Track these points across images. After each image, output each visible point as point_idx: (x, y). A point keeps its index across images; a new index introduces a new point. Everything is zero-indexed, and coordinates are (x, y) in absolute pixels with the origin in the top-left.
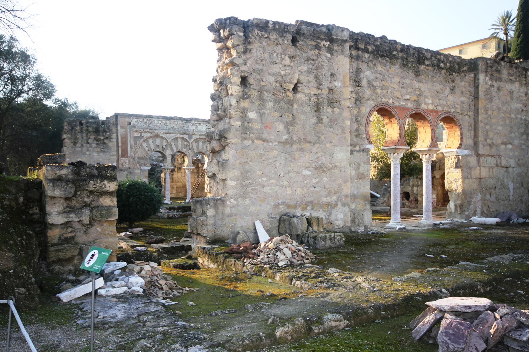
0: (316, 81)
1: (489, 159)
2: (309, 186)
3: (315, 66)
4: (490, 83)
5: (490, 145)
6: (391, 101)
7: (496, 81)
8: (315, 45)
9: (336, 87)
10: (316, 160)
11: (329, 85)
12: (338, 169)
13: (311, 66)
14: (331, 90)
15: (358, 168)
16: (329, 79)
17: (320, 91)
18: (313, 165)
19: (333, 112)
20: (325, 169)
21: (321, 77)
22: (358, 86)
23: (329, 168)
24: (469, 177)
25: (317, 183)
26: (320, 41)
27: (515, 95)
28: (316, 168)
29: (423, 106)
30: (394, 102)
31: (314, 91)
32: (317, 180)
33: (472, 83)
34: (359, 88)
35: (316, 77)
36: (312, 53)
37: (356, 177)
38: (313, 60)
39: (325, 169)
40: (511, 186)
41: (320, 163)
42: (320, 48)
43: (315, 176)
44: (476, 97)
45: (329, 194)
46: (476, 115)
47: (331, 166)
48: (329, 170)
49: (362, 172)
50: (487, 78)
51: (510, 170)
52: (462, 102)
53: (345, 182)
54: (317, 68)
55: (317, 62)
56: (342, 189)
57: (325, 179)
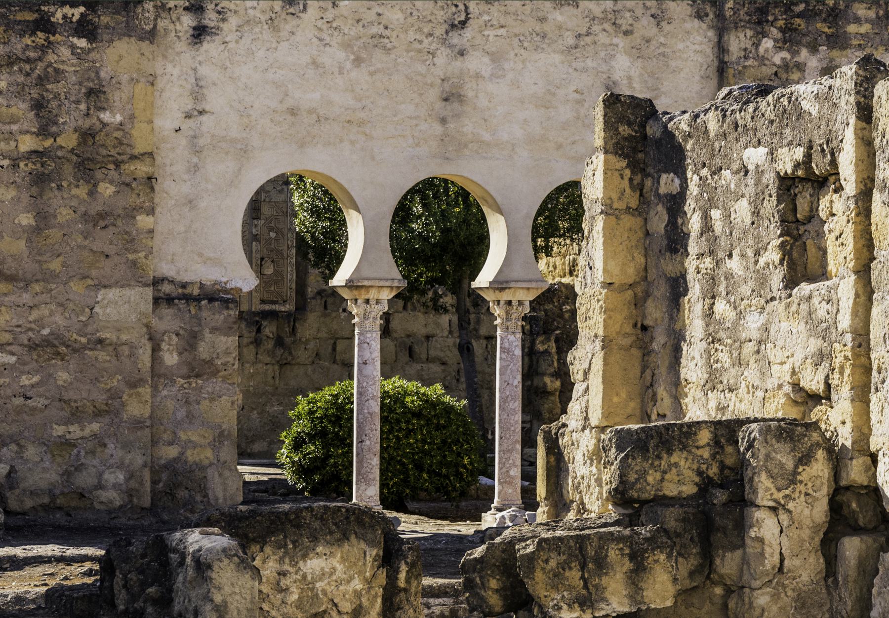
0: (37, 115)
3: (35, 75)
8: (36, 21)
11: (80, 123)
12: (111, 349)
13: (21, 79)
14: (87, 135)
16: (83, 107)
17: (48, 143)
18: (24, 339)
19: (92, 193)
21: (54, 104)
23: (77, 346)
25: (33, 386)
26: (52, 9)
28: (33, 347)
32: (36, 379)
35: (38, 106)
36: (21, 44)
37: (185, 370)
38: (28, 61)
41: (46, 332)
42: (53, 24)
43: (27, 368)
45: (76, 416)
47: (84, 340)
48: (75, 351)
54: (41, 81)
55: (40, 66)
56: (123, 405)
57: (63, 376)
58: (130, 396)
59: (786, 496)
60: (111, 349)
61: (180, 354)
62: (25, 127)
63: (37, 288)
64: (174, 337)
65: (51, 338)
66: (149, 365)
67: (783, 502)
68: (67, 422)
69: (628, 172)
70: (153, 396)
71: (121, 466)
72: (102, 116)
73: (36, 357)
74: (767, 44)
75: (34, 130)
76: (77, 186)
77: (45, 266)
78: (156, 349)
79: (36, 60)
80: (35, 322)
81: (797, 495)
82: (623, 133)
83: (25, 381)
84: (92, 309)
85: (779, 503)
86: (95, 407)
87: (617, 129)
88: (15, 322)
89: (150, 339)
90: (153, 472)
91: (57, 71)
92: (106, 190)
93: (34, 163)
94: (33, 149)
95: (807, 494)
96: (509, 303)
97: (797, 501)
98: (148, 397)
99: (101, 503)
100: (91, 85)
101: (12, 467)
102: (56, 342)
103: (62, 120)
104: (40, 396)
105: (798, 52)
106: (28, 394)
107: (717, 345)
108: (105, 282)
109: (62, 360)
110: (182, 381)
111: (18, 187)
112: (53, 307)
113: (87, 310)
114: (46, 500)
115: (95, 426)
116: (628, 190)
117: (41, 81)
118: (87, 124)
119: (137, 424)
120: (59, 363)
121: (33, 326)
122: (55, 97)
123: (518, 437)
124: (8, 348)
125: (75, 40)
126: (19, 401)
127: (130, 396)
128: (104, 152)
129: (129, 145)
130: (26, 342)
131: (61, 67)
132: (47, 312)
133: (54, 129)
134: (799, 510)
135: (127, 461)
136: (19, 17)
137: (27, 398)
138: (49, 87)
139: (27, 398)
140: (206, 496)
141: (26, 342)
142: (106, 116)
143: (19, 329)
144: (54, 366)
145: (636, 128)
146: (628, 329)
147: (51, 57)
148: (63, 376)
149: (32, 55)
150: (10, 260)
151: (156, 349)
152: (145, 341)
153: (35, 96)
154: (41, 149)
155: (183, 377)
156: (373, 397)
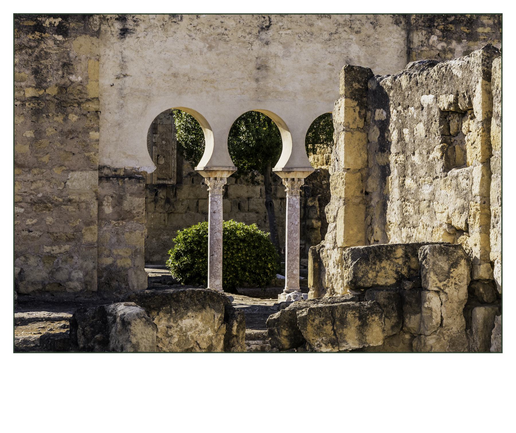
0: (35, 77)
3: (34, 55)
8: (35, 26)
11: (59, 81)
12: (75, 205)
13: (26, 57)
14: (63, 88)
16: (60, 72)
17: (41, 92)
18: (28, 199)
19: (65, 120)
20: (49, 205)
21: (45, 71)
23: (57, 203)
25: (33, 225)
28: (33, 203)
32: (35, 221)
35: (36, 72)
37: (116, 216)
38: (30, 47)
39: (49, 205)
41: (40, 195)
42: (44, 28)
43: (30, 215)
45: (57, 241)
47: (61, 200)
48: (56, 206)
49: (127, 208)
54: (38, 59)
55: (37, 50)
56: (82, 235)
58: (86, 230)
59: (444, 285)
60: (75, 205)
61: (113, 207)
62: (29, 84)
63: (35, 171)
64: (110, 198)
65: (43, 198)
66: (96, 213)
67: (442, 288)
68: (52, 245)
69: (358, 108)
70: (99, 230)
71: (81, 268)
72: (71, 77)
73: (34, 209)
74: (434, 38)
75: (34, 85)
76: (57, 116)
77: (39, 160)
78: (100, 205)
79: (35, 47)
80: (34, 190)
81: (450, 284)
82: (355, 87)
83: (29, 222)
84: (65, 183)
85: (440, 289)
86: (67, 236)
87: (352, 85)
88: (23, 190)
89: (97, 199)
90: (99, 271)
91: (46, 53)
92: (73, 118)
93: (33, 103)
94: (33, 95)
95: (455, 284)
96: (293, 180)
97: (450, 287)
98: (96, 231)
99: (70, 288)
100: (65, 61)
101: (22, 269)
102: (46, 201)
103: (49, 80)
104: (37, 230)
105: (451, 43)
106: (31, 229)
107: (406, 203)
108: (72, 168)
109: (49, 210)
110: (115, 222)
111: (25, 116)
112: (44, 182)
113: (63, 183)
114: (40, 287)
115: (67, 247)
116: (358, 118)
117: (38, 59)
118: (62, 82)
119: (90, 246)
120: (47, 212)
121: (33, 192)
122: (45, 67)
123: (298, 253)
124: (19, 204)
125: (56, 36)
126: (25, 233)
127: (86, 230)
128: (72, 97)
130: (29, 201)
131: (49, 51)
132: (41, 185)
133: (44, 85)
134: (451, 293)
135: (84, 266)
136: (26, 24)
137: (30, 231)
138: (42, 62)
139: (30, 231)
140: (127, 285)
141: (29, 201)
142: (73, 78)
143: (26, 194)
144: (44, 214)
145: (362, 84)
146: (358, 194)
147: (43, 46)
148: (49, 220)
149: (33, 44)
150: (20, 156)
151: (100, 205)
152: (94, 200)
153: (34, 67)
154: (37, 96)
155: (114, 220)
156: (219, 231)
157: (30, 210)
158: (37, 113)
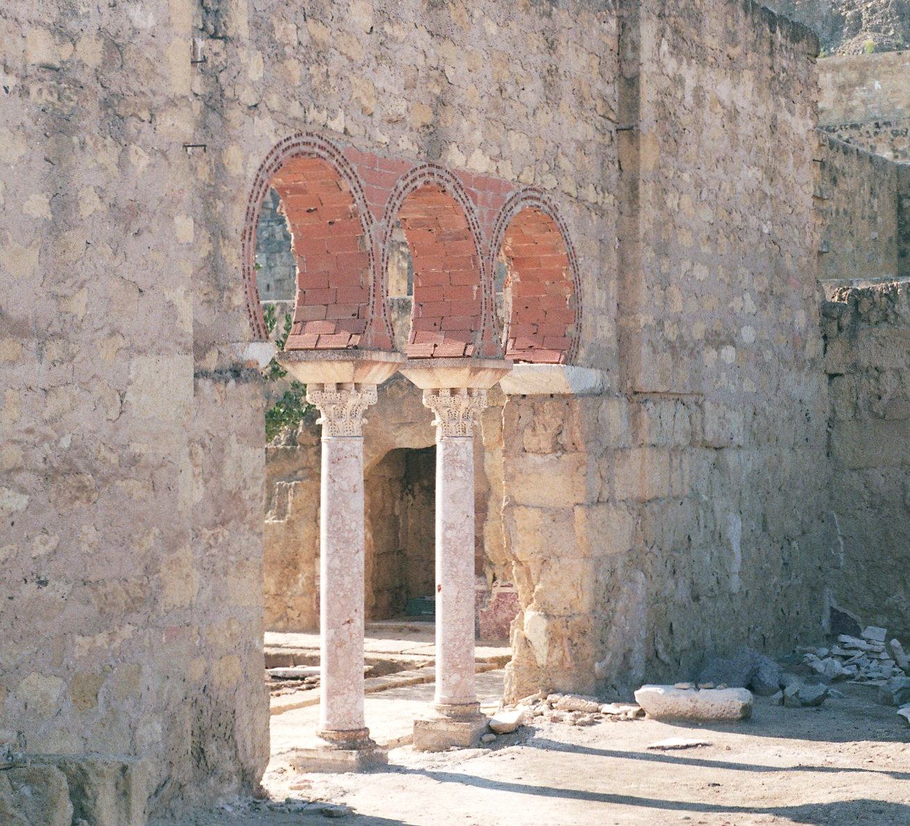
1: (667, 409)
2: (18, 575)
4: (671, 65)
5: (671, 346)
6: (337, 125)
7: (689, 64)
9: (136, 32)
10: (49, 430)
14: (114, 47)
15: (218, 466)
17: (66, 51)
18: (37, 455)
19: (122, 164)
22: (214, 36)
23: (105, 470)
24: (606, 494)
27: (745, 129)
28: (49, 476)
29: (454, 158)
30: (353, 129)
31: (41, 49)
32: (53, 542)
33: (611, 60)
34: (218, 45)
40: (735, 530)
41: (65, 443)
44: (629, 131)
46: (626, 206)
49: (231, 485)
50: (665, 47)
51: (731, 458)
52: (581, 147)
53: (173, 547)
62: (35, 15)
77: (63, 307)
80: (50, 422)
86: (127, 592)
92: (140, 161)
102: (80, 465)
104: (58, 578)
108: (139, 343)
110: (207, 533)
111: (29, 137)
126: (29, 590)
129: (164, 78)
139: (43, 583)
141: (41, 466)
143: (31, 438)
157: (41, 499)
158: (60, 126)
